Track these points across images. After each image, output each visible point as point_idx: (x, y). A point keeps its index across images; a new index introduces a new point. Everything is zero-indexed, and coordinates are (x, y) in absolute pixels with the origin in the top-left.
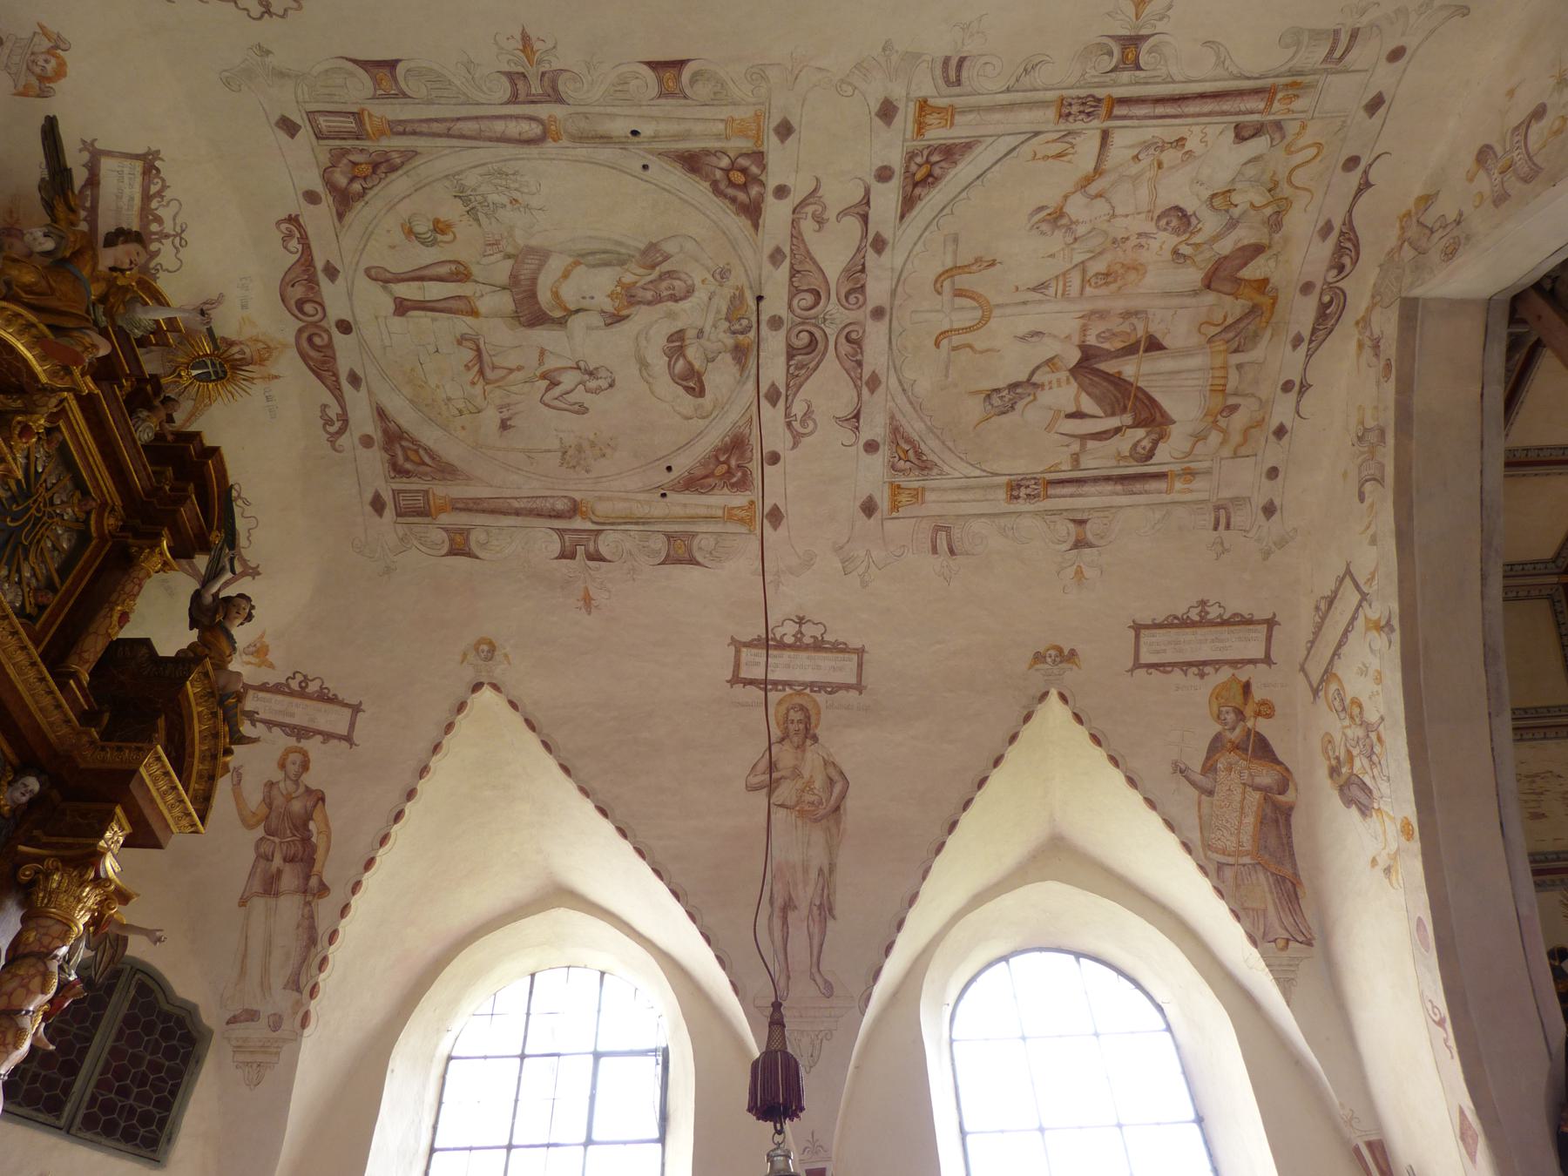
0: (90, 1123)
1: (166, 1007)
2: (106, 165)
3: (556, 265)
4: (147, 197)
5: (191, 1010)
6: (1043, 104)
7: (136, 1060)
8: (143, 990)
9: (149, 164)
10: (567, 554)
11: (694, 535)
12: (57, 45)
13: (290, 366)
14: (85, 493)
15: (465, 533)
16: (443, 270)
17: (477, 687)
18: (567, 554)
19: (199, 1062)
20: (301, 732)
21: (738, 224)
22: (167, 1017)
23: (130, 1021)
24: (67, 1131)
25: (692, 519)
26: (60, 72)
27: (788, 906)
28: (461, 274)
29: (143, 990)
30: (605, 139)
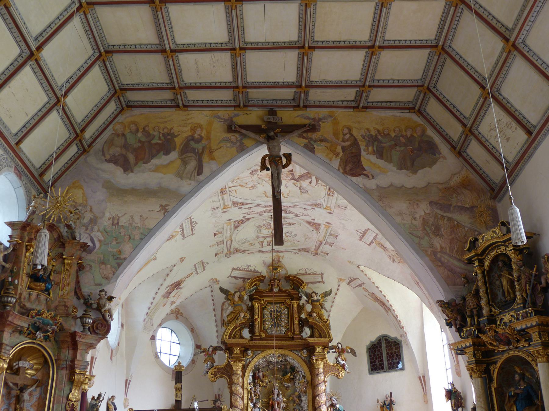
0: (389, 368)
1: (391, 341)
2: (232, 275)
3: (259, 235)
4: (240, 270)
5: (396, 338)
6: (223, 198)
7: (392, 353)
8: (386, 340)
9: (233, 269)
10: (332, 246)
11: (330, 233)
12: (212, 279)
13: (281, 254)
14: (281, 303)
15: (322, 252)
16: (261, 243)
17: (359, 267)
18: (332, 246)
19: (402, 347)
20: (360, 285)
21: (251, 220)
22: (392, 342)
23: (387, 347)
24: (386, 371)
25: (326, 231)
26: (216, 279)
27: (418, 283)
28: (263, 242)
29: (386, 340)
30: (231, 236)
